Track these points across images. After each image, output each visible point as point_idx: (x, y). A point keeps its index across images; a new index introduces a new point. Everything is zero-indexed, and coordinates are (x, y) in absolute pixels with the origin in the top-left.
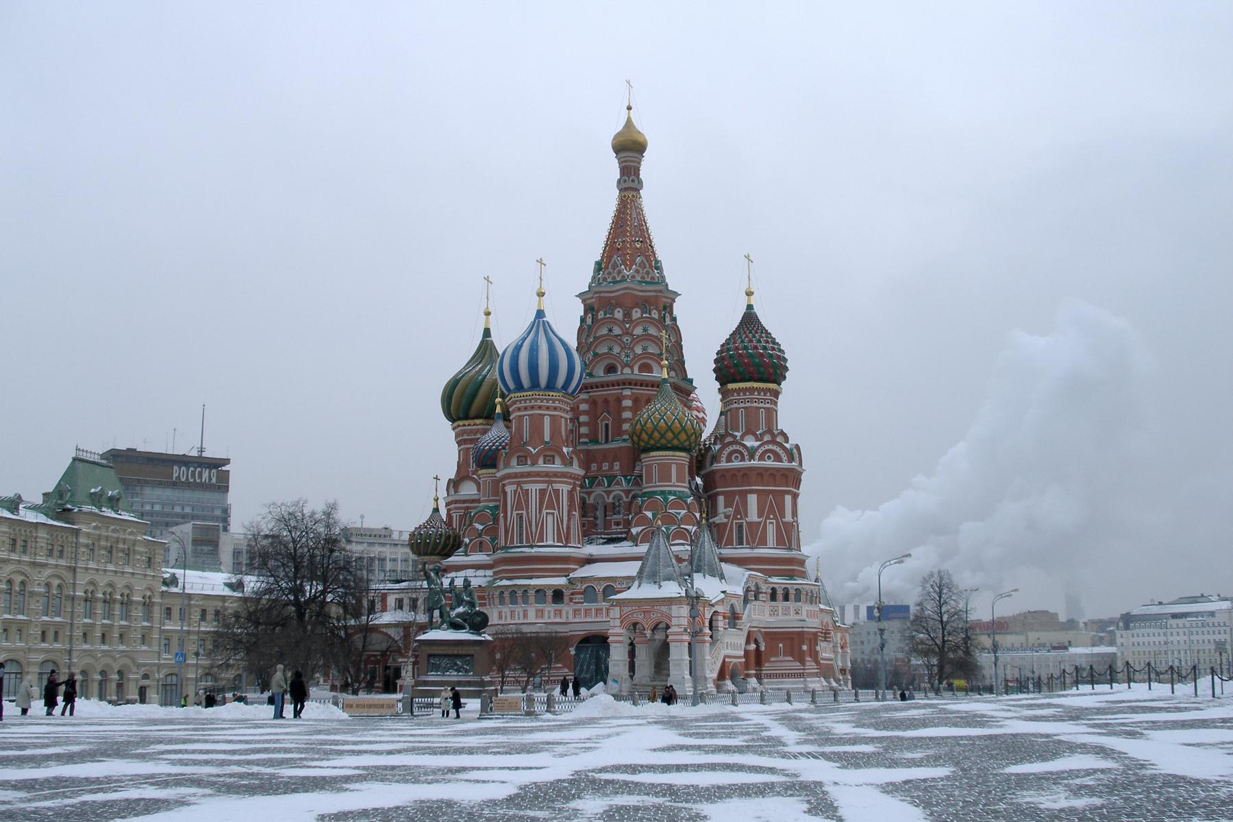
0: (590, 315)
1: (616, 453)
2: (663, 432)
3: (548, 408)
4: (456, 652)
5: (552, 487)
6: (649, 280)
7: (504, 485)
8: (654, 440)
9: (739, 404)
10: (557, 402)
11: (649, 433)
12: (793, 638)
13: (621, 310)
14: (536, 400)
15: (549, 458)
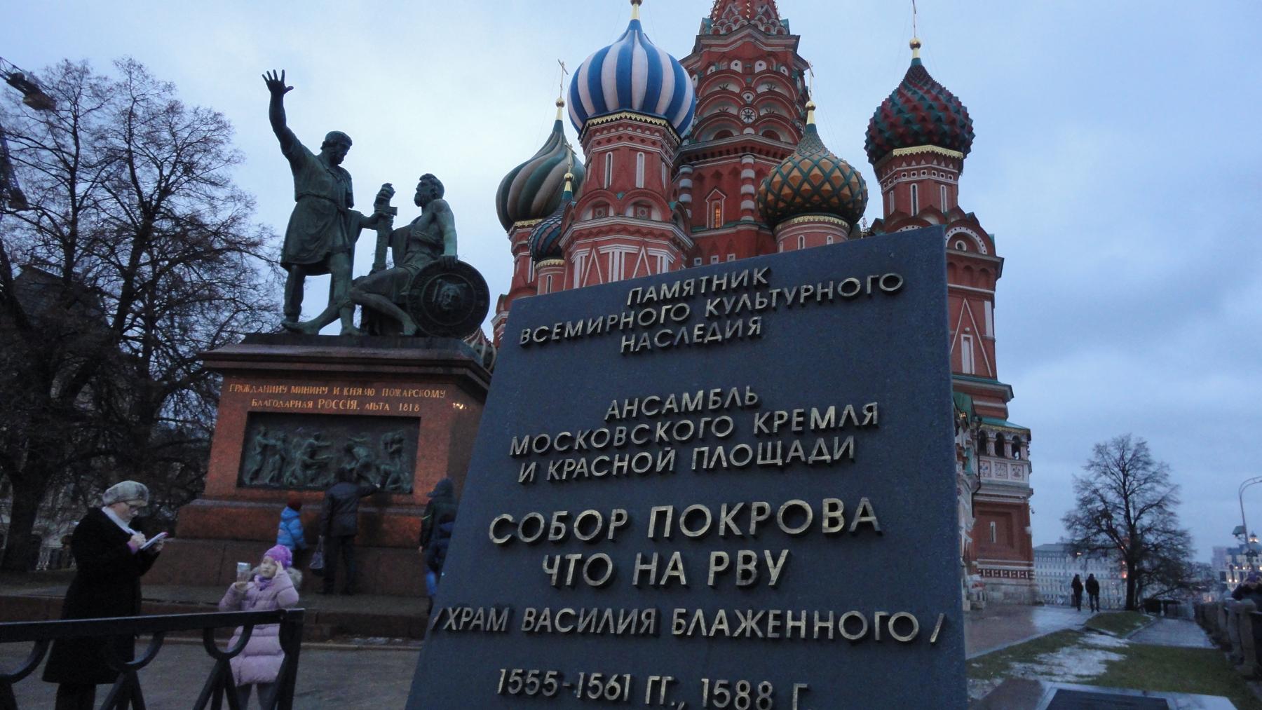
0: (696, 76)
1: (731, 240)
2: (817, 184)
3: (643, 141)
4: (353, 405)
5: (647, 254)
6: (775, 33)
7: (570, 254)
8: (802, 196)
9: (909, 176)
10: (657, 134)
11: (795, 187)
12: (1010, 514)
13: (739, 63)
14: (627, 126)
15: (643, 209)
